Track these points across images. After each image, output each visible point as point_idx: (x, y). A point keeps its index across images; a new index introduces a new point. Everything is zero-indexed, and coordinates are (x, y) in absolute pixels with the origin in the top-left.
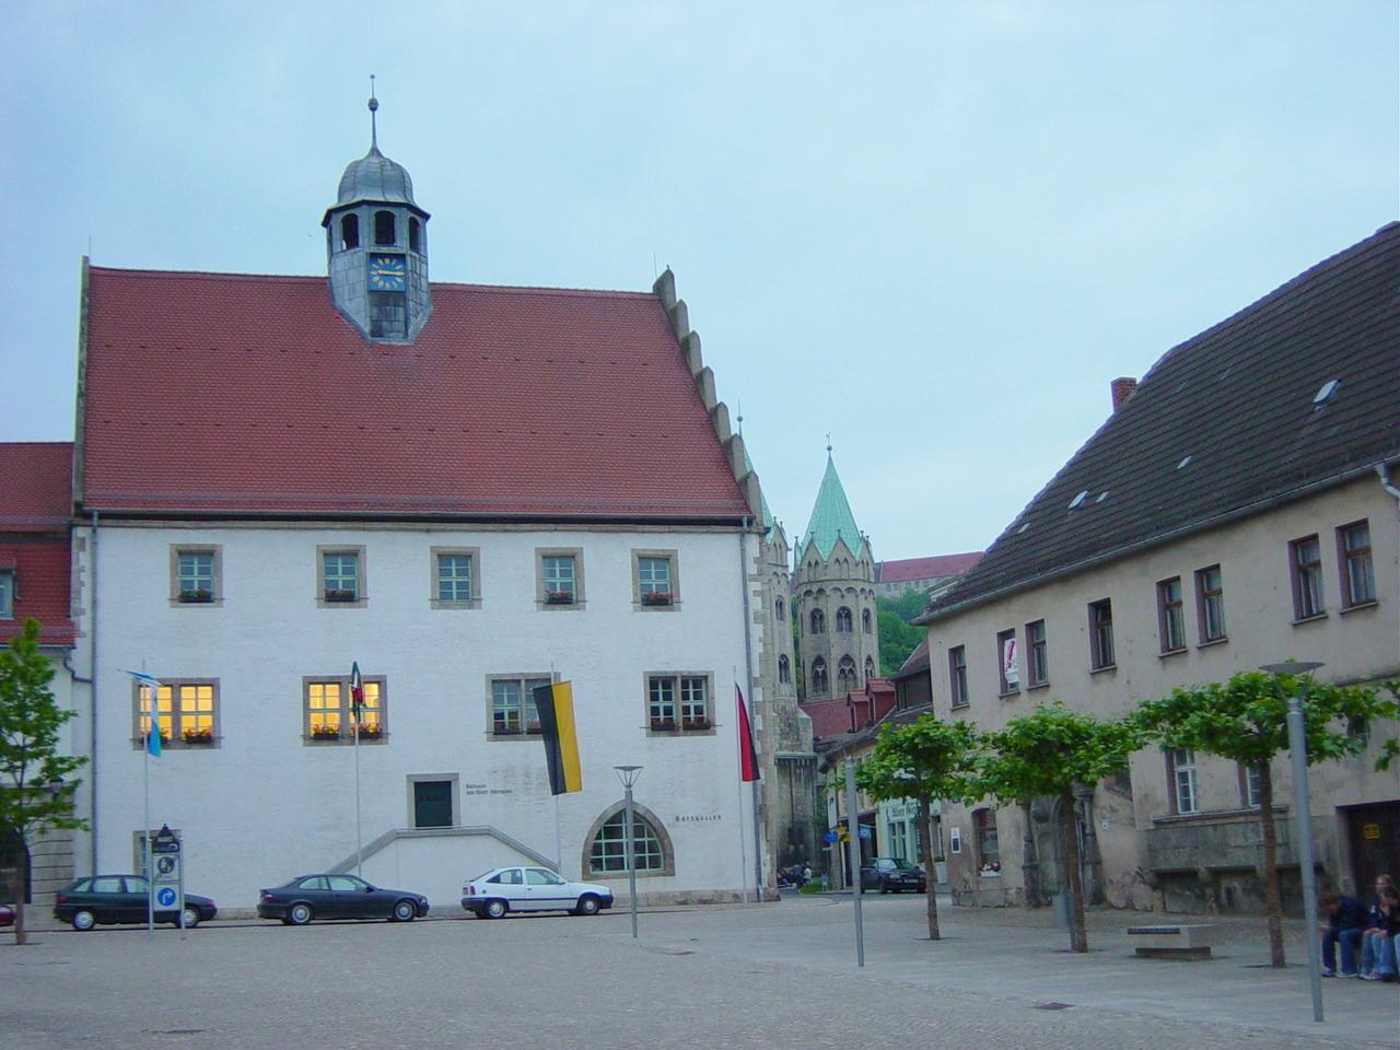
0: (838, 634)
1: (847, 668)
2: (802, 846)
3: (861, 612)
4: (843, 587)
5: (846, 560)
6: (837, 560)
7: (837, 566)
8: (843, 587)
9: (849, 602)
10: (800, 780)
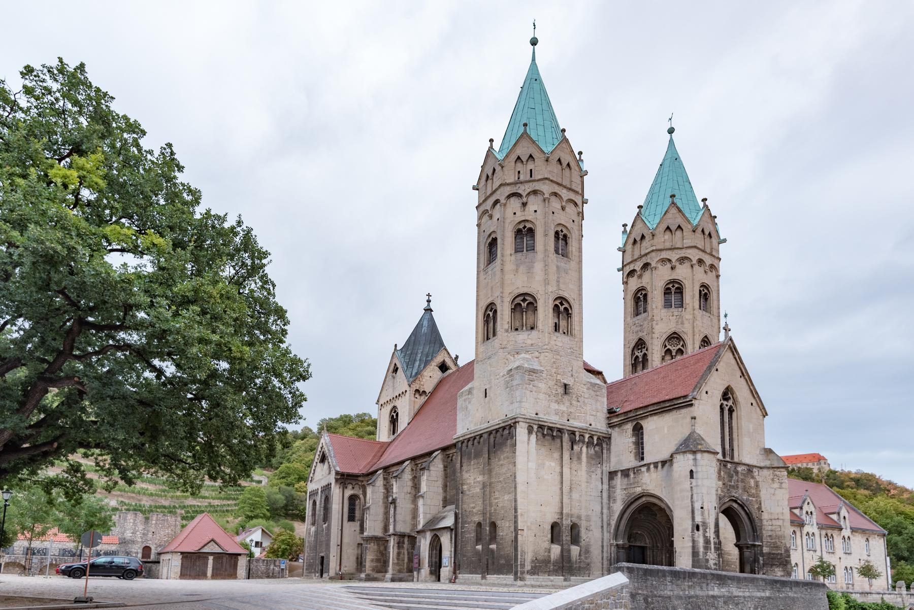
2: (575, 550)
5: (679, 227)
6: (668, 228)
7: (668, 235)
8: (674, 256)
10: (579, 458)
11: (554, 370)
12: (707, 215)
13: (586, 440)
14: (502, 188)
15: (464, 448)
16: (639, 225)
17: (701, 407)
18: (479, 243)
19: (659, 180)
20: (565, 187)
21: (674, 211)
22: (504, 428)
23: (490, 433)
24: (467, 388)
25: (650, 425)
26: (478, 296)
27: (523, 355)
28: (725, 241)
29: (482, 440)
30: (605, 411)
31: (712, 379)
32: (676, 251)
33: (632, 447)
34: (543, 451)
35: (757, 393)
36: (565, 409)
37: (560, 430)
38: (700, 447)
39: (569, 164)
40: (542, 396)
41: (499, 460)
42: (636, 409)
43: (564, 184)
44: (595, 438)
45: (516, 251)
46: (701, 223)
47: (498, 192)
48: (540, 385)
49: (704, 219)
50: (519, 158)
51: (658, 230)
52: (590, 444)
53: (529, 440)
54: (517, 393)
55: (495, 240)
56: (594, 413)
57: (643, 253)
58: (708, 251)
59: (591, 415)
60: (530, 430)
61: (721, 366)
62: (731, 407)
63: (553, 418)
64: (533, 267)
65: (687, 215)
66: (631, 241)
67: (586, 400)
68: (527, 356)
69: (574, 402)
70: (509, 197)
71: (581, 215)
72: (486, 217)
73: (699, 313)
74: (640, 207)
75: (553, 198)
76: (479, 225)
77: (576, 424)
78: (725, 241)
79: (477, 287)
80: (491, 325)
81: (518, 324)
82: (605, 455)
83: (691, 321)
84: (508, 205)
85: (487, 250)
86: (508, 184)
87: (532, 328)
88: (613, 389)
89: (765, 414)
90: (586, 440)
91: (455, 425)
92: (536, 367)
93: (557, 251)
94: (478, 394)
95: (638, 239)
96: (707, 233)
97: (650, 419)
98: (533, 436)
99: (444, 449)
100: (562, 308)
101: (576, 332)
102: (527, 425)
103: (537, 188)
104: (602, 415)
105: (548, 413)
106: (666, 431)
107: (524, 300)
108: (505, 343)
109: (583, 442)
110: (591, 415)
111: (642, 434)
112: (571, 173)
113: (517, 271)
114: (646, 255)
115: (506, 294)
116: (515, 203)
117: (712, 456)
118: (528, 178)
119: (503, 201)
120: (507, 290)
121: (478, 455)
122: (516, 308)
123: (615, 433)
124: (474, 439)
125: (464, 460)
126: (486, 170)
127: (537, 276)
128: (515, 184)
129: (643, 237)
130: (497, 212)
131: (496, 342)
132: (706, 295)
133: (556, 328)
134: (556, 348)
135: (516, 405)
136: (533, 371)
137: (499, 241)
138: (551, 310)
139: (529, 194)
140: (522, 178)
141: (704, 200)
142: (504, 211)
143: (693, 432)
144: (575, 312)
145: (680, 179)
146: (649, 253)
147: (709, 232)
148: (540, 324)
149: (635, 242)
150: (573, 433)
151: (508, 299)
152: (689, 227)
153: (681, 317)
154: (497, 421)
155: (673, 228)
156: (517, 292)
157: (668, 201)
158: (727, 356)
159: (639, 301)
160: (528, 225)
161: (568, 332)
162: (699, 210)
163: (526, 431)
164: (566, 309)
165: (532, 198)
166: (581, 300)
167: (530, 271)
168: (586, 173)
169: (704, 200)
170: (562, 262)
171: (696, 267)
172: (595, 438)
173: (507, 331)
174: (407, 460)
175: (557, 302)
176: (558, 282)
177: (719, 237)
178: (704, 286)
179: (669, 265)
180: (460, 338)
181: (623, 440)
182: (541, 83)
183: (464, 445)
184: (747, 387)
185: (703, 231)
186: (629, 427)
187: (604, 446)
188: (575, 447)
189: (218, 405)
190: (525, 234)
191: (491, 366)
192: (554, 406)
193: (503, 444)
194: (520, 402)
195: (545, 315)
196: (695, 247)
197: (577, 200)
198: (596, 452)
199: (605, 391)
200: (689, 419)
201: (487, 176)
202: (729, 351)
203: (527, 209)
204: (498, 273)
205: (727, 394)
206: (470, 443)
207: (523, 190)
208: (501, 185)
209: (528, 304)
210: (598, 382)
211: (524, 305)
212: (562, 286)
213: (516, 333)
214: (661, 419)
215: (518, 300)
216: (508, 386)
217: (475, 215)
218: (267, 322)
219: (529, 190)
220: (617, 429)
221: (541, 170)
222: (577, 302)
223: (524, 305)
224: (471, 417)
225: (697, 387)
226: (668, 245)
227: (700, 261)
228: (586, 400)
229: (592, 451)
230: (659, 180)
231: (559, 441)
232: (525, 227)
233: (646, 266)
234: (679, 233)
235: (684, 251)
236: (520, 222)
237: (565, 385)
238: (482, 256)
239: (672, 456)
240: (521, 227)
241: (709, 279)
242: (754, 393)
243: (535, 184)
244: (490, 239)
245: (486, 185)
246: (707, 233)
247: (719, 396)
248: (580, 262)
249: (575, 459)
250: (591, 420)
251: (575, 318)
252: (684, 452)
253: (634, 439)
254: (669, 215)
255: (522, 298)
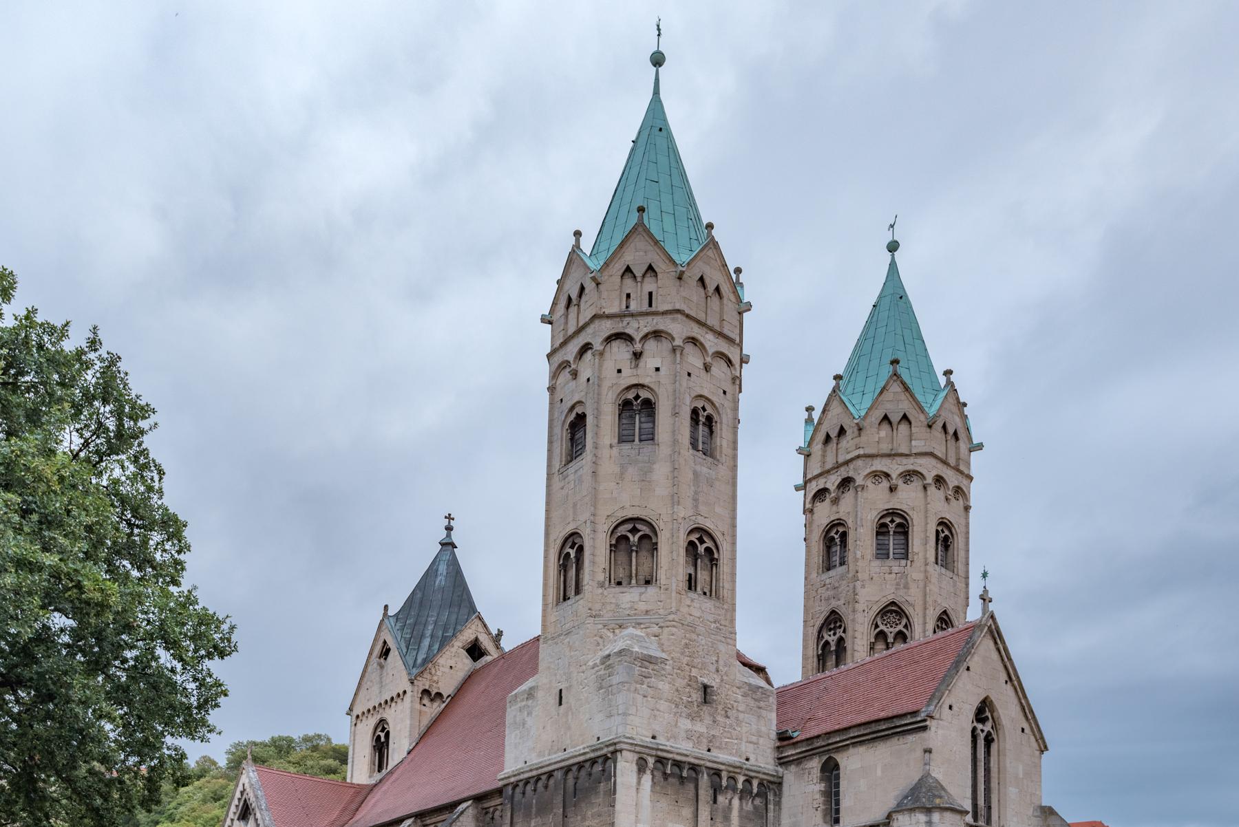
0: (878, 562)
1: (891, 631)
3: (932, 527)
4: (895, 468)
5: (905, 417)
7: (885, 431)
8: (895, 468)
9: (908, 498)
10: (727, 818)
11: (685, 660)
12: (951, 400)
13: (740, 786)
14: (597, 322)
15: (518, 796)
16: (836, 409)
17: (940, 732)
18: (551, 421)
19: (871, 334)
20: (711, 329)
21: (896, 387)
22: (593, 761)
23: (568, 770)
24: (525, 687)
25: (852, 762)
26: (548, 519)
27: (631, 630)
28: (980, 447)
29: (552, 781)
30: (773, 735)
31: (960, 684)
32: (898, 459)
33: (820, 799)
34: (664, 804)
35: (1032, 711)
36: (703, 729)
37: (694, 768)
38: (937, 801)
39: (720, 290)
40: (663, 705)
41: (584, 819)
42: (829, 734)
43: (709, 323)
44: (755, 783)
45: (621, 441)
46: (943, 414)
47: (590, 330)
48: (661, 685)
49: (947, 405)
50: (628, 269)
51: (868, 420)
52: (745, 794)
53: (639, 783)
54: (620, 699)
55: (581, 418)
56: (754, 739)
57: (841, 460)
58: (952, 462)
59: (749, 743)
60: (641, 767)
61: (975, 661)
62: (989, 734)
63: (683, 747)
64: (651, 471)
65: (920, 398)
66: (821, 437)
67: (741, 716)
68: (638, 632)
69: (720, 718)
70: (609, 339)
71: (737, 381)
72: (565, 375)
73: (934, 570)
74: (838, 378)
75: (689, 348)
76: (552, 389)
77: (723, 757)
78: (980, 447)
79: (548, 503)
80: (572, 573)
81: (621, 574)
82: (771, 814)
83: (921, 584)
84: (607, 355)
85: (566, 435)
86: (609, 317)
87: (648, 582)
88: (786, 696)
89: (1043, 748)
90: (740, 786)
91: (503, 755)
92: (655, 652)
93: (694, 445)
94: (546, 699)
95: (833, 434)
96: (951, 431)
97: (852, 750)
98: (647, 779)
99: (479, 799)
100: (701, 549)
101: (725, 593)
102: (636, 757)
103: (661, 327)
104: (768, 743)
105: (675, 737)
106: (879, 773)
107: (634, 531)
108: (598, 606)
109: (734, 789)
110: (749, 743)
111: (838, 777)
112: (722, 304)
113: (622, 476)
114: (847, 463)
115: (601, 519)
116: (620, 352)
117: (958, 817)
118: (645, 307)
119: (597, 345)
120: (604, 511)
121: (543, 809)
122: (619, 543)
123: (790, 776)
124: (539, 780)
125: (519, 820)
126: (566, 287)
127: (655, 485)
128: (621, 316)
129: (842, 431)
130: (587, 368)
131: (578, 605)
132: (946, 539)
133: (691, 583)
134: (690, 619)
135: (617, 720)
136: (648, 660)
137: (590, 420)
138: (682, 552)
139: (645, 337)
140: (634, 307)
141: (948, 373)
142: (601, 366)
143: (927, 775)
144: (724, 556)
145: (907, 333)
146: (851, 460)
147: (955, 433)
148: (662, 575)
149: (828, 438)
150: (717, 773)
151: (604, 527)
152: (922, 417)
153: (904, 575)
154: (580, 749)
155: (895, 418)
156: (622, 515)
157: (887, 370)
158: (985, 646)
159: (832, 543)
160: (644, 394)
161: (712, 592)
162: (939, 390)
163: (635, 768)
164: (708, 550)
165: (651, 345)
166: (734, 536)
167: (645, 479)
168: (749, 307)
169: (948, 373)
170: (704, 467)
171: (932, 490)
172: (755, 783)
173: (601, 585)
174: (408, 817)
175: (694, 537)
176: (696, 500)
177: (970, 439)
178: (944, 523)
179: (885, 484)
180: (511, 594)
181: (802, 789)
182: (670, 138)
183: (518, 790)
184: (1016, 701)
185: (944, 427)
186: (815, 764)
187: (771, 797)
188: (720, 798)
189: (51, 697)
190: (637, 408)
191: (571, 648)
192: (685, 724)
193: (593, 790)
194: (625, 714)
195: (671, 559)
196: (932, 454)
197: (731, 359)
198: (755, 807)
199: (773, 700)
200: (919, 753)
201: (568, 300)
202: (989, 637)
203: (641, 364)
204: (588, 479)
205: (984, 711)
206: (530, 788)
207: (637, 328)
208: (595, 317)
209: (641, 538)
210: (763, 683)
211: (634, 539)
212: (703, 509)
213: (618, 589)
214: (871, 751)
215: (623, 530)
216: (603, 686)
217: (543, 370)
218: (145, 542)
219: (646, 330)
220: (793, 768)
221: (669, 295)
222: (728, 538)
223: (634, 539)
224: (530, 742)
225: (935, 697)
226: (885, 448)
227: (939, 480)
228: (741, 716)
229: (749, 806)
230: (871, 334)
231: (691, 786)
232: (637, 397)
233: (846, 482)
234: (903, 427)
235: (912, 460)
236: (629, 388)
237: (705, 687)
238: (557, 445)
239: (889, 816)
240: (631, 395)
241: (952, 513)
242: (1027, 711)
243: (657, 319)
244: (573, 416)
245: (566, 316)
246: (951, 431)
247: (971, 715)
248: (734, 468)
249: (719, 819)
250: (747, 749)
251: (724, 566)
252: (912, 810)
253: (822, 786)
254: (888, 396)
255: (630, 526)
